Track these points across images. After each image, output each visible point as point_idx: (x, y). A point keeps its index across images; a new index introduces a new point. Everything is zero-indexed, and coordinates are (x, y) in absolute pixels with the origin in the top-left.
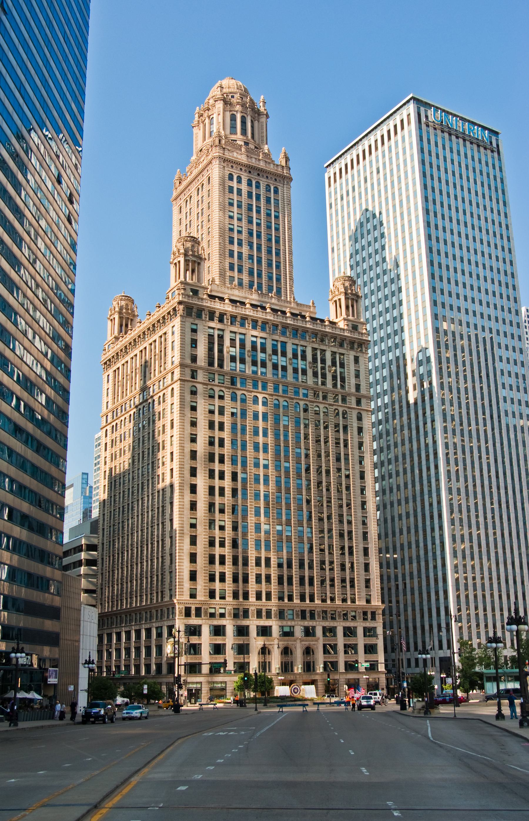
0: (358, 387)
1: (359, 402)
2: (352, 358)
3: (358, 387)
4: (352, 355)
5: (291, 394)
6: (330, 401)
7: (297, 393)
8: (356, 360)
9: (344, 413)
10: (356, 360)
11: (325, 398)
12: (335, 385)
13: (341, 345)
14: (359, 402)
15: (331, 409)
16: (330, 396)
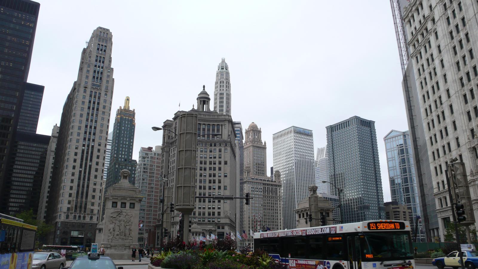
0: (280, 195)
1: (280, 198)
2: (278, 189)
3: (280, 195)
4: (278, 188)
5: (267, 197)
6: (274, 198)
7: (268, 197)
8: (279, 189)
9: (277, 201)
10: (279, 189)
11: (273, 198)
12: (275, 195)
13: (277, 186)
14: (280, 198)
15: (274, 200)
16: (274, 197)
